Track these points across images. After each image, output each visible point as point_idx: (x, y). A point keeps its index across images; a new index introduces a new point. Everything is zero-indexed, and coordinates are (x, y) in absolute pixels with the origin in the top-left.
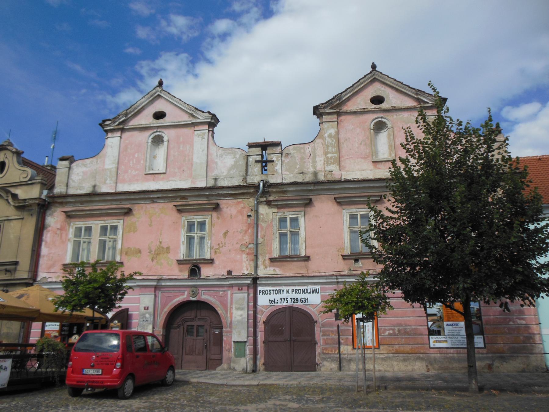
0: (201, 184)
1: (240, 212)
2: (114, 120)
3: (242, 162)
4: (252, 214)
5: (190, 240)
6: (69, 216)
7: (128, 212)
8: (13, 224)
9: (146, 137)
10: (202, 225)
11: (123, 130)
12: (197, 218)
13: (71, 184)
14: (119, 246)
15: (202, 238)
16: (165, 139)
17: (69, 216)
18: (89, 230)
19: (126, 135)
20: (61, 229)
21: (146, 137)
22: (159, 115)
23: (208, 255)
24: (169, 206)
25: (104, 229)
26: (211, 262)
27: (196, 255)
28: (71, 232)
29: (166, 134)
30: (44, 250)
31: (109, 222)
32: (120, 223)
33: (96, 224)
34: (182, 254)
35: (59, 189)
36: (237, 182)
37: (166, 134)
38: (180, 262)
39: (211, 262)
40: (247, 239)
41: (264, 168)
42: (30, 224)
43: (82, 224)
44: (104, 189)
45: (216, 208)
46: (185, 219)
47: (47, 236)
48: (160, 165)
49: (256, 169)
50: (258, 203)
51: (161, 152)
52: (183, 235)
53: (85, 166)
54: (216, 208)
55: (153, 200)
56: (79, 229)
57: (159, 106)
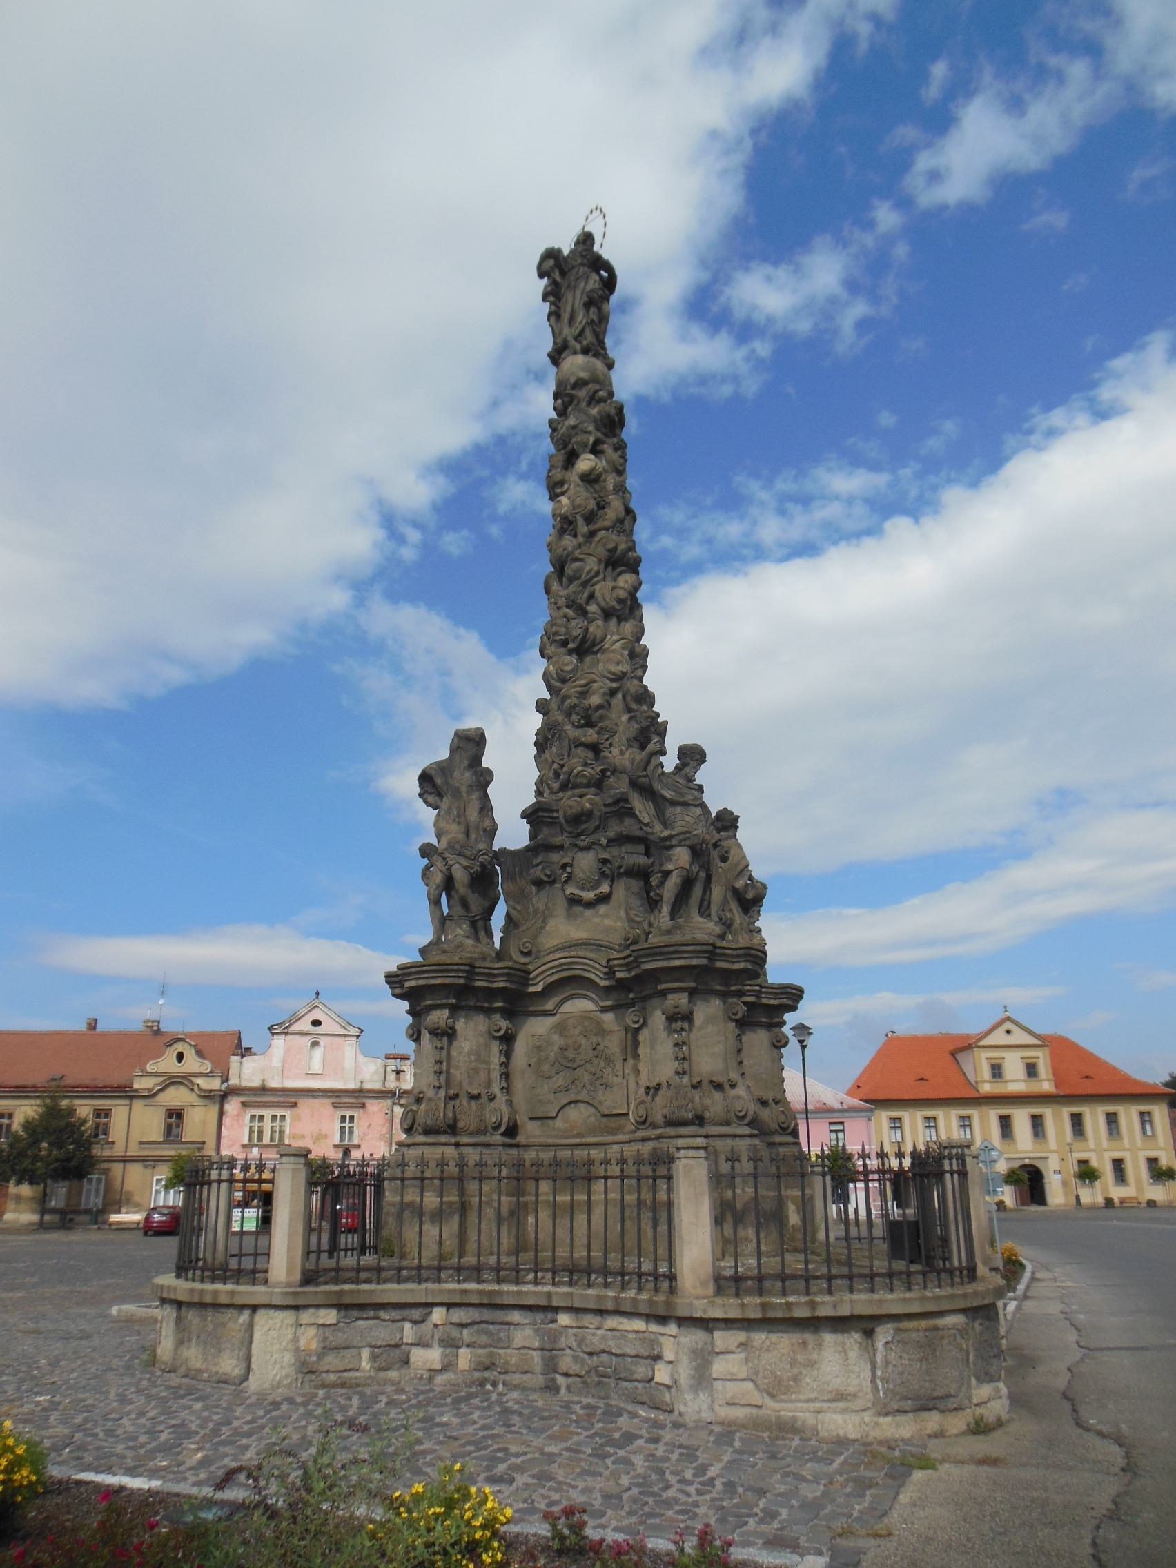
0: (351, 1085)
1: (380, 1110)
2: (280, 1024)
3: (382, 1070)
4: (389, 1112)
5: (343, 1128)
6: (244, 1104)
7: (295, 1105)
8: (196, 1109)
9: (307, 1041)
10: (352, 1118)
11: (286, 1033)
12: (348, 1113)
13: (244, 1077)
14: (287, 1131)
15: (351, 1129)
16: (322, 1044)
17: (244, 1104)
18: (262, 1118)
19: (289, 1037)
20: (238, 1115)
21: (307, 1041)
22: (316, 1023)
23: (356, 1142)
24: (328, 1102)
25: (274, 1117)
26: (358, 1146)
27: (346, 1142)
28: (248, 1118)
29: (323, 1041)
30: (224, 1132)
31: (279, 1112)
32: (288, 1113)
33: (268, 1113)
34: (337, 1141)
35: (233, 1081)
36: (377, 1086)
37: (322, 1041)
38: (335, 1146)
39: (358, 1146)
40: (384, 1130)
41: (398, 1079)
42: (214, 1110)
43: (257, 1112)
44: (274, 1084)
45: (363, 1106)
46: (339, 1113)
47: (227, 1121)
48: (316, 1066)
49: (392, 1076)
50: (394, 1104)
51: (318, 1053)
52: (338, 1125)
53: (254, 1061)
54: (363, 1106)
55: (314, 1097)
56: (253, 1117)
57: (316, 1015)
